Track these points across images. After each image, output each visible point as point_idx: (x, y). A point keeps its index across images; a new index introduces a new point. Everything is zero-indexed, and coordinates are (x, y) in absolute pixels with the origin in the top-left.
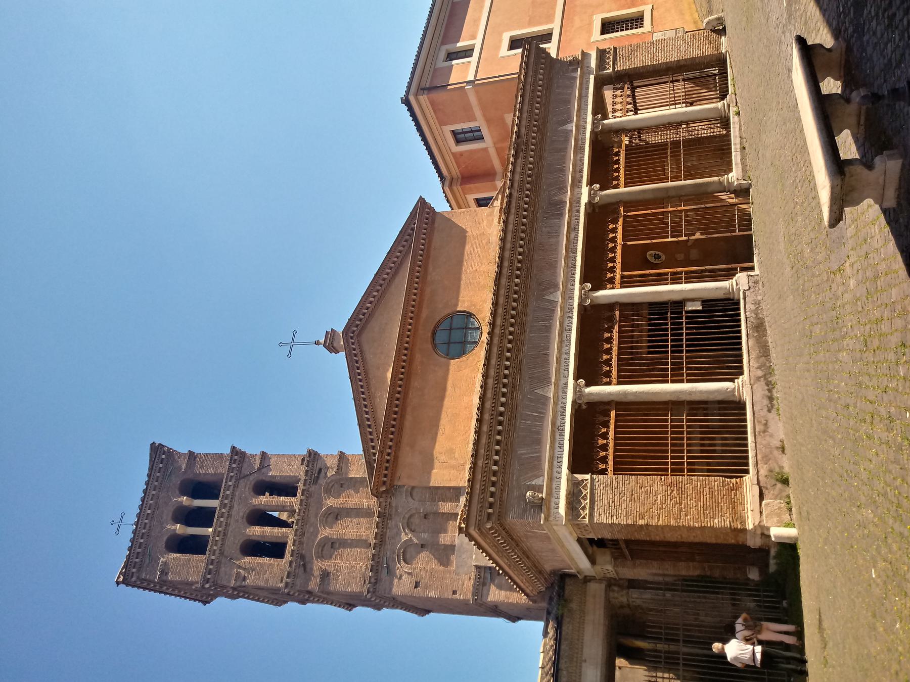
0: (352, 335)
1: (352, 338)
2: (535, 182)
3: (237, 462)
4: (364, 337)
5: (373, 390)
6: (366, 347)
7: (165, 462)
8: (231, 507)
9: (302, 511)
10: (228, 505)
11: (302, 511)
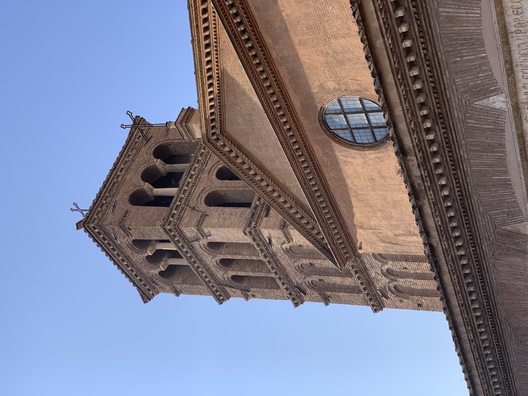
0: (215, 137)
1: (217, 140)
2: (462, 210)
3: (177, 234)
4: (229, 129)
5: (281, 181)
6: (241, 141)
7: (101, 232)
8: (201, 261)
9: (274, 266)
10: (197, 260)
11: (274, 266)
